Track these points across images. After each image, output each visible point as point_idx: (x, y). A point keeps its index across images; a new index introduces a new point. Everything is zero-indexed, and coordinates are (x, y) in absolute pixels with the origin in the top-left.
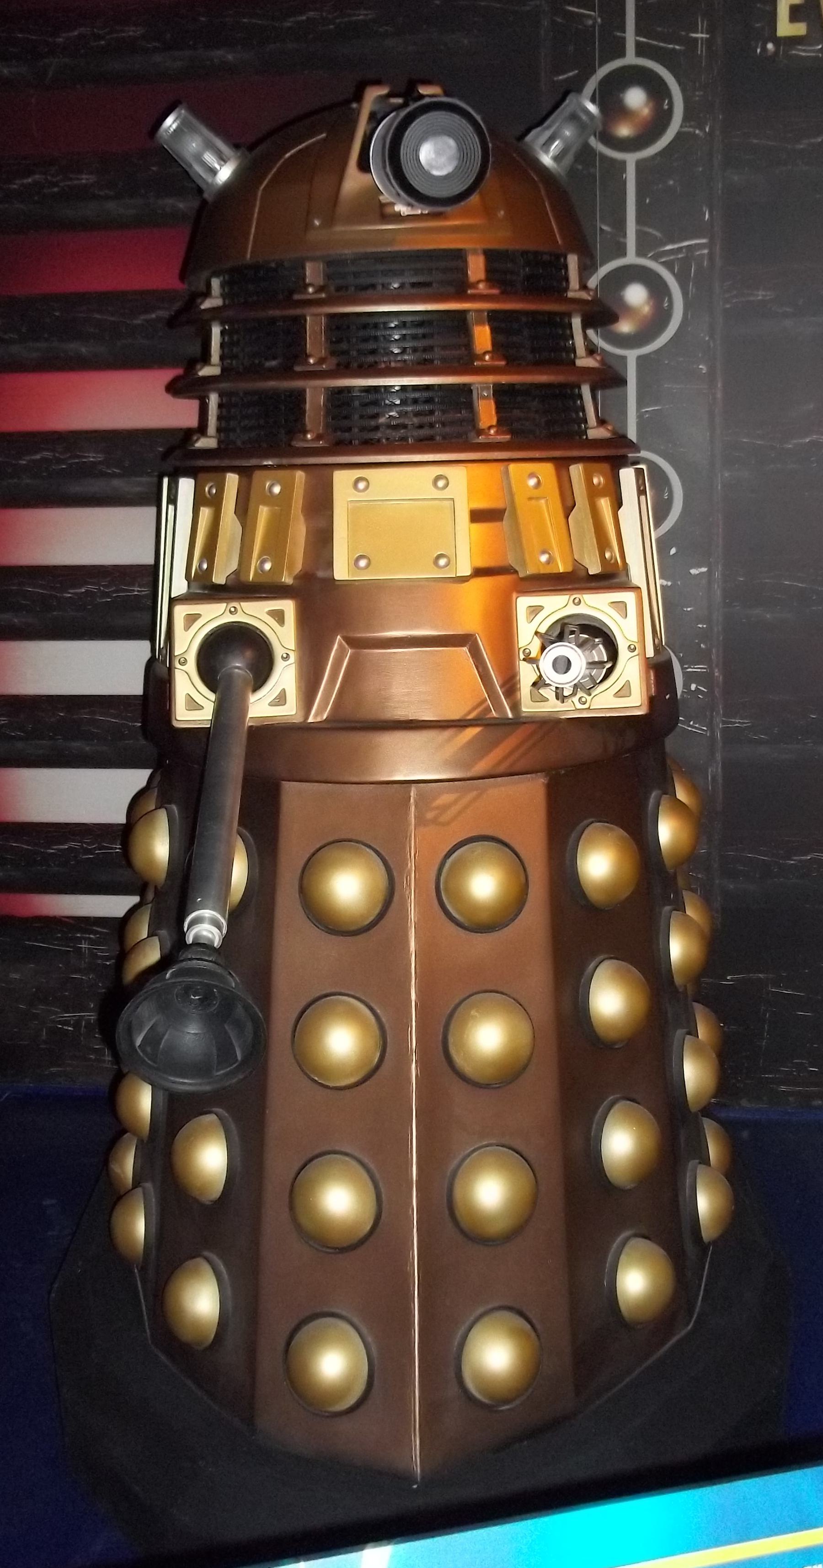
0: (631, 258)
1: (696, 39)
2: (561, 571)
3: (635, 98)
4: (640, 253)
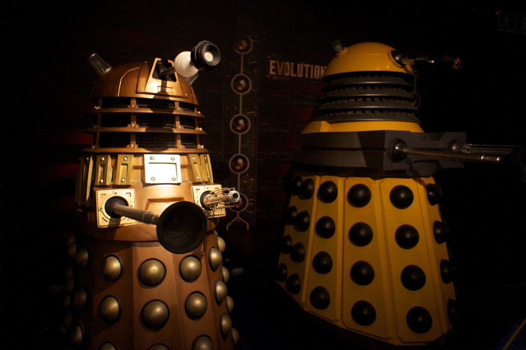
0: (240, 114)
2: (119, 184)
3: (242, 82)
4: (243, 113)
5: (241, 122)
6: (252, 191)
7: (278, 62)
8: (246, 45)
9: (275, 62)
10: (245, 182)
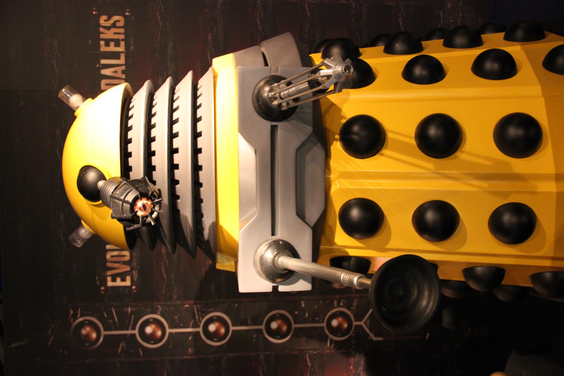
1: (131, 311)
3: (149, 330)
4: (199, 327)
5: (212, 328)
6: (321, 302)
7: (109, 273)
8: (88, 329)
9: (109, 278)
10: (307, 315)
